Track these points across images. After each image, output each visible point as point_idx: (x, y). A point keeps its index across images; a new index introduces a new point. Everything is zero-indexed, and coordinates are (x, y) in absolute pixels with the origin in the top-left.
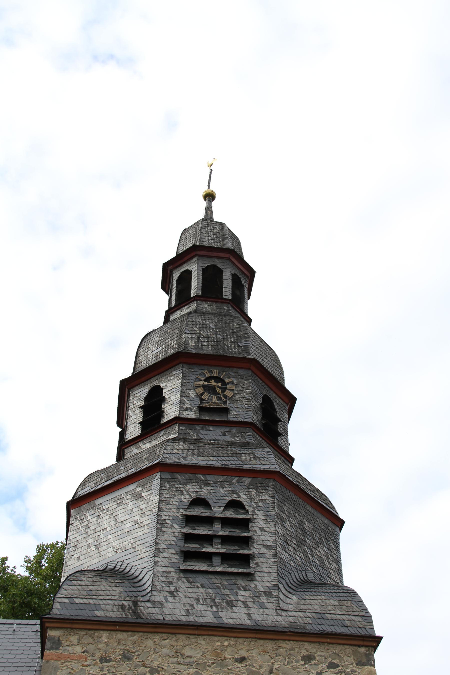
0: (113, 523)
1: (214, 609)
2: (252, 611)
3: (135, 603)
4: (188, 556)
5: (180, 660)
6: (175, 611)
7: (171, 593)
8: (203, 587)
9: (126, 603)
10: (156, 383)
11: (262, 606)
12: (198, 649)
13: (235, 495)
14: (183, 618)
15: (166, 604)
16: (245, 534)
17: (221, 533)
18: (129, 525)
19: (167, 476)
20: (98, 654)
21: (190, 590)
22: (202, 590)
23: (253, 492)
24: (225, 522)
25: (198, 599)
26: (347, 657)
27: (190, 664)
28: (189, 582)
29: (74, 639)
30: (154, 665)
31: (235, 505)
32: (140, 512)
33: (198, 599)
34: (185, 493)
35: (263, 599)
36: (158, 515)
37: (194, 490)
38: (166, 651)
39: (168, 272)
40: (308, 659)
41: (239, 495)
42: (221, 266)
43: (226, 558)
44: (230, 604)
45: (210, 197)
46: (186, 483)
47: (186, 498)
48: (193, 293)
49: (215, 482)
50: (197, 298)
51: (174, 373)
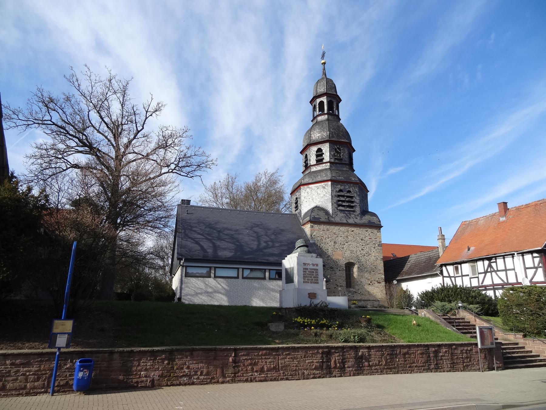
4: (339, 205)
6: (337, 220)
10: (319, 147)
12: (343, 229)
24: (348, 197)
26: (375, 231)
31: (349, 192)
37: (339, 187)
40: (367, 231)
42: (333, 100)
43: (348, 206)
44: (350, 218)
47: (338, 190)
48: (326, 112)
50: (326, 114)
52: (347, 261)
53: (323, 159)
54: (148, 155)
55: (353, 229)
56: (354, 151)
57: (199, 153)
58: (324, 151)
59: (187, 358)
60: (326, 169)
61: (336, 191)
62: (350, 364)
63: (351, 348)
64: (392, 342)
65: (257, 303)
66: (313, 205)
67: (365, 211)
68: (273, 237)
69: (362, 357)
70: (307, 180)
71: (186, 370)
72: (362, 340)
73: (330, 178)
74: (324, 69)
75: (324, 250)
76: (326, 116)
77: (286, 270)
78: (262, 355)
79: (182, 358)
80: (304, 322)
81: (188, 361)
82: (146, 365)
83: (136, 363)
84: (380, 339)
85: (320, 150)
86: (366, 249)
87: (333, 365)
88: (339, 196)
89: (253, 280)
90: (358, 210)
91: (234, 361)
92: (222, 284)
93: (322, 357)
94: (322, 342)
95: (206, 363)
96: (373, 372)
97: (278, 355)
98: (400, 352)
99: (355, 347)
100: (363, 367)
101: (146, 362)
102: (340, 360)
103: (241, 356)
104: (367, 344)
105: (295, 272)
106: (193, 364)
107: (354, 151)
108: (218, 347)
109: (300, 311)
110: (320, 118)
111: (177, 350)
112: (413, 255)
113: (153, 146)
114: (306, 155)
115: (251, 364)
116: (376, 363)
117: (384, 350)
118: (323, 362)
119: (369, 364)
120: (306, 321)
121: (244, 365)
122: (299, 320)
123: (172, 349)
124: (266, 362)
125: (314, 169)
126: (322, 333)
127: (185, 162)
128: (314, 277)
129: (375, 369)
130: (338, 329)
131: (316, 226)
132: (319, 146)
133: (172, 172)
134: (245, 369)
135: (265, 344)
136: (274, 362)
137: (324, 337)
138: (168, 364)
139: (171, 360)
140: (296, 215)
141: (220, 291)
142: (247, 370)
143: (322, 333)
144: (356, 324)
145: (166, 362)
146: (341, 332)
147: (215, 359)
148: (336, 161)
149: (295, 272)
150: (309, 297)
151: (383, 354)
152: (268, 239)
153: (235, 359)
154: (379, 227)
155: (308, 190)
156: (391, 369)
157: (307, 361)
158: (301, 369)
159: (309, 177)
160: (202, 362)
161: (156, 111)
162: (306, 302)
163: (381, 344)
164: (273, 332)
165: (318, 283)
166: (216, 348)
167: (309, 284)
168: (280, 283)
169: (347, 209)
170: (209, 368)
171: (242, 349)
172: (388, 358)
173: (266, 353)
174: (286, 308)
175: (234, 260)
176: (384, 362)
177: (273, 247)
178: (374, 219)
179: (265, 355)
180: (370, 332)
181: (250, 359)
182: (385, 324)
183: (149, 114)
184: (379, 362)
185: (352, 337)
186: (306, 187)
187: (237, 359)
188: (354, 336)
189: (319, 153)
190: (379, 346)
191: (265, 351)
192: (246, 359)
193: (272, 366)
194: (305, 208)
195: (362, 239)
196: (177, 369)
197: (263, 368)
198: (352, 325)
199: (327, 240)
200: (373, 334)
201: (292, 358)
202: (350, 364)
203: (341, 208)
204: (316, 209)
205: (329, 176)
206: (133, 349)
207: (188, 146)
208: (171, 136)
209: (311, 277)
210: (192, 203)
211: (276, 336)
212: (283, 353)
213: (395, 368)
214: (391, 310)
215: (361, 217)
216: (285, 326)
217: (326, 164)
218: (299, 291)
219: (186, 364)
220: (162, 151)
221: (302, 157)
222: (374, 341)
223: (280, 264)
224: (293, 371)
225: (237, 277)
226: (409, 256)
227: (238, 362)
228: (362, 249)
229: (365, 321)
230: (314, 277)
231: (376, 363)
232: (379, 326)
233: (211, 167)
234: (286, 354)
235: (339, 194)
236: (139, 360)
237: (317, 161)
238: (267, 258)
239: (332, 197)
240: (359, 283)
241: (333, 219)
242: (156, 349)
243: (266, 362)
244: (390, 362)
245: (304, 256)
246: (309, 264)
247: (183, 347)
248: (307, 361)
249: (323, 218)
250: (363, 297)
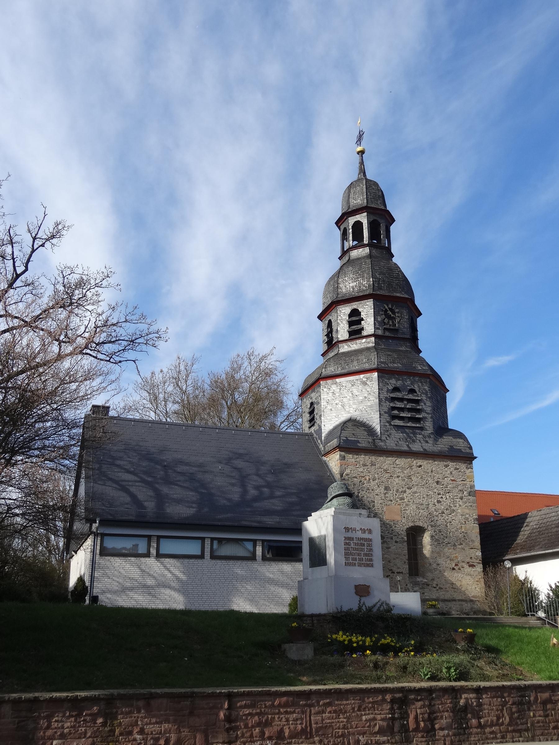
0: (351, 395)
2: (423, 444)
3: (374, 440)
4: (394, 417)
6: (391, 444)
9: (370, 440)
10: (355, 307)
11: (427, 442)
12: (401, 462)
14: (395, 448)
16: (418, 407)
17: (408, 407)
18: (361, 398)
19: (380, 374)
20: (361, 463)
22: (401, 434)
24: (410, 401)
29: (351, 456)
30: (385, 468)
31: (412, 391)
32: (367, 392)
33: (400, 439)
37: (393, 382)
38: (389, 462)
40: (446, 466)
42: (379, 220)
43: (411, 419)
44: (414, 441)
46: (389, 379)
47: (390, 388)
48: (366, 241)
51: (368, 303)
52: (411, 524)
53: (362, 329)
54: (37, 318)
55: (420, 462)
56: (420, 314)
57: (134, 317)
58: (363, 315)
59: (139, 712)
60: (368, 349)
61: (388, 391)
62: (444, 722)
63: (445, 690)
64: (519, 680)
65: (241, 605)
66: (344, 416)
67: (442, 429)
68: (270, 478)
69: (466, 709)
70: (331, 370)
71: (138, 737)
72: (463, 676)
73: (375, 366)
74: (362, 163)
75: (366, 502)
76: (367, 250)
77: (312, 540)
78: (280, 705)
79: (130, 712)
80: (350, 641)
81: (141, 718)
82: (63, 727)
83: (43, 723)
84: (495, 673)
85: (355, 313)
86: (447, 501)
87: (412, 725)
88: (393, 399)
89: (231, 562)
90: (429, 425)
91: (229, 719)
92: (173, 570)
93: (392, 709)
94: (388, 679)
95: (175, 722)
96: (487, 738)
97: (310, 706)
98: (536, 698)
99: (453, 689)
100: (468, 728)
101: (62, 721)
102: (426, 716)
103: (242, 707)
104: (475, 684)
105: (330, 543)
106: (150, 723)
107: (420, 314)
108: (196, 690)
109: (341, 620)
110: (355, 254)
111: (121, 697)
112: (535, 513)
113: (45, 301)
114: (330, 322)
115: (259, 724)
116: (492, 721)
117: (506, 695)
118: (393, 719)
119: (480, 723)
120: (354, 639)
121: (246, 726)
122: (341, 637)
123: (112, 695)
124: (287, 720)
125: (344, 348)
126: (387, 663)
127: (105, 334)
128: (366, 555)
129: (492, 733)
130: (415, 656)
131: (350, 457)
132: (354, 305)
133: (81, 353)
134: (248, 734)
135: (282, 684)
136: (302, 719)
137: (391, 671)
138: (104, 724)
139: (110, 716)
140: (311, 435)
141: (173, 584)
142: (251, 736)
143: (387, 663)
144: (446, 646)
145: (100, 720)
146: (423, 660)
147: (191, 714)
148: (387, 334)
149: (330, 543)
150: (357, 593)
151: (506, 703)
152: (261, 482)
153: (230, 714)
154: (468, 458)
155: (334, 387)
156: (519, 731)
157: (364, 718)
158: (353, 734)
159: (334, 364)
160: (167, 721)
161: (53, 237)
162: (351, 603)
163: (500, 684)
164: (294, 662)
165: (372, 566)
166: (194, 693)
167: (357, 567)
168: (299, 566)
169: (409, 424)
170: (180, 732)
171: (243, 694)
172: (514, 710)
173: (287, 701)
174: (312, 616)
175: (203, 523)
176: (508, 719)
177: (272, 497)
178: (459, 444)
179: (286, 705)
180: (474, 660)
181: (257, 714)
182: (502, 645)
183: (38, 243)
184: (498, 718)
185: (444, 670)
186: (329, 381)
187: (234, 713)
188: (449, 668)
189: (354, 319)
190: (498, 687)
191: (284, 699)
192: (249, 714)
193: (299, 727)
194: (329, 421)
195: (438, 483)
196: (121, 734)
197: (281, 731)
198: (440, 647)
199: (372, 483)
200: (481, 663)
201: (335, 711)
202: (444, 722)
204: (349, 424)
205: (374, 362)
206: (37, 694)
207: (113, 304)
208: (80, 284)
209: (358, 555)
210: (112, 413)
211: (299, 669)
212: (318, 702)
213: (527, 730)
214: (505, 618)
215: (436, 440)
216: (316, 650)
217: (369, 340)
218: (336, 579)
219: (137, 725)
220: (62, 314)
221: (320, 327)
222: (485, 678)
223: (298, 530)
224: (339, 737)
225: (202, 557)
226: (525, 516)
227: (235, 721)
228: (439, 502)
229: (465, 639)
230: (366, 555)
231: (492, 721)
232: (490, 649)
233: (157, 343)
234: (324, 704)
235: (393, 395)
236: (49, 718)
237: (351, 333)
238: (259, 518)
239: (380, 400)
240: (434, 566)
241: (382, 444)
242: (83, 694)
243: (287, 720)
244: (518, 718)
245: (344, 514)
246: (355, 530)
247: (131, 691)
248: (364, 718)
249: (364, 441)
250: (442, 595)
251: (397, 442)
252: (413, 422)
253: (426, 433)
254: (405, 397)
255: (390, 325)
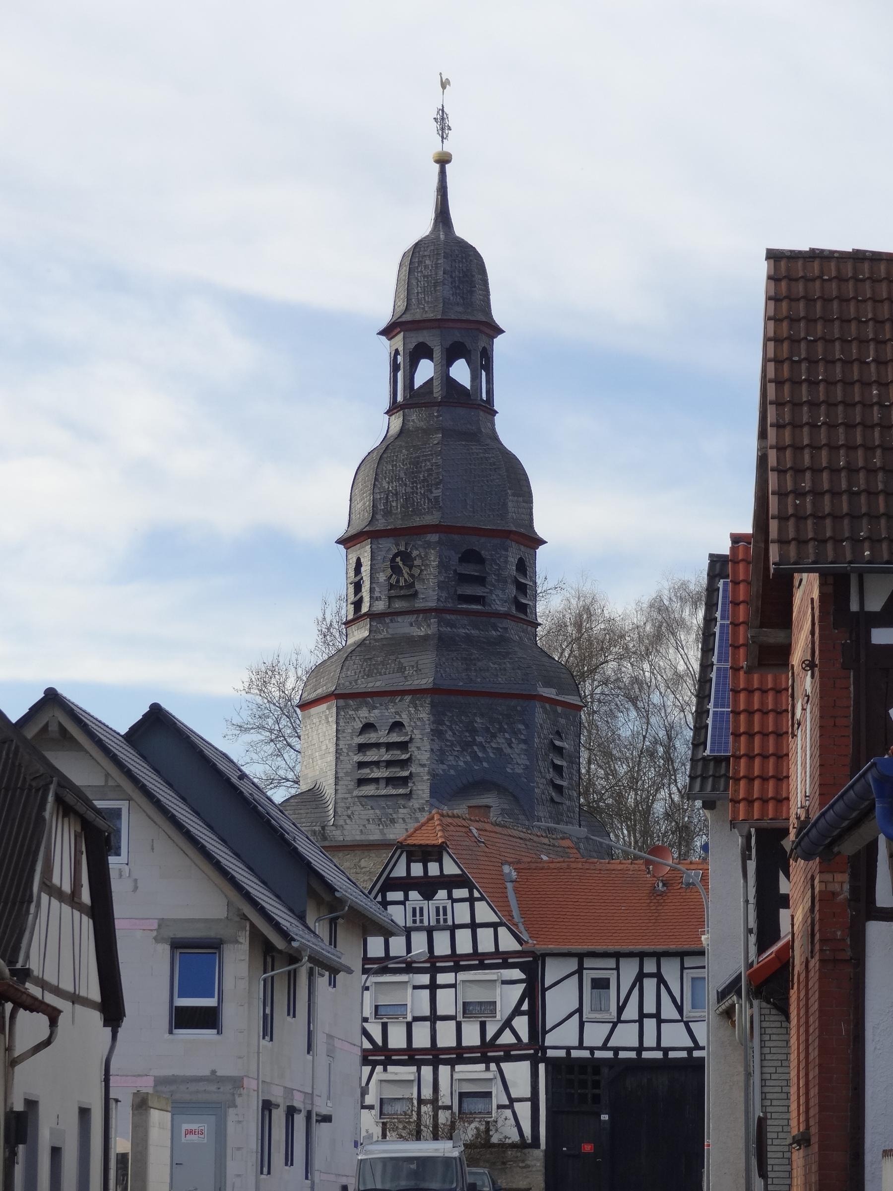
1: (381, 827)
3: (323, 828)
4: (361, 782)
5: (358, 870)
7: (349, 817)
8: (372, 809)
9: (317, 828)
13: (397, 717)
14: (358, 838)
15: (345, 827)
19: (342, 702)
21: (362, 812)
22: (372, 812)
23: (412, 710)
24: (389, 746)
25: (368, 820)
27: (364, 873)
28: (363, 806)
31: (397, 726)
33: (368, 820)
34: (357, 719)
35: (418, 815)
36: (337, 745)
37: (365, 714)
39: (4, 1017)
41: (400, 716)
43: (389, 781)
44: (393, 821)
45: (443, 161)
46: (356, 710)
47: (359, 725)
49: (381, 705)
148: (398, 605)
203: (370, 790)
235: (362, 740)
239: (338, 752)
251: (364, 826)
252: (395, 787)
253: (415, 803)
254: (381, 741)
255: (401, 588)
